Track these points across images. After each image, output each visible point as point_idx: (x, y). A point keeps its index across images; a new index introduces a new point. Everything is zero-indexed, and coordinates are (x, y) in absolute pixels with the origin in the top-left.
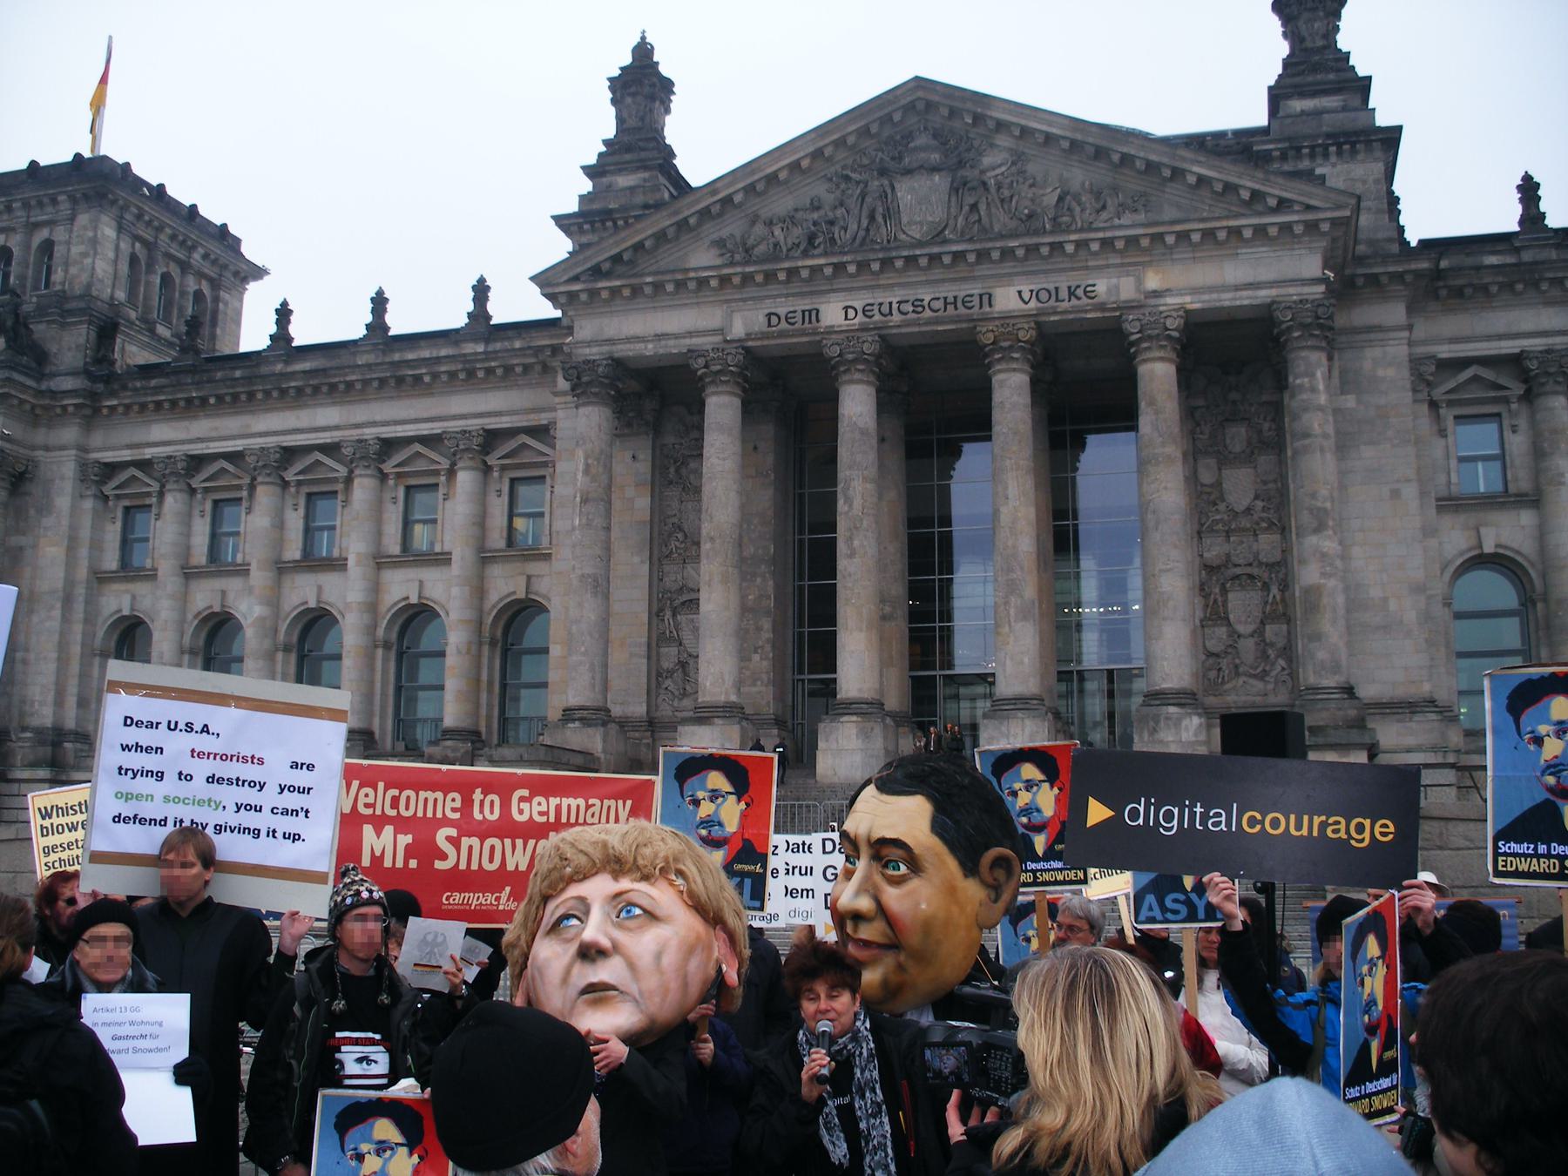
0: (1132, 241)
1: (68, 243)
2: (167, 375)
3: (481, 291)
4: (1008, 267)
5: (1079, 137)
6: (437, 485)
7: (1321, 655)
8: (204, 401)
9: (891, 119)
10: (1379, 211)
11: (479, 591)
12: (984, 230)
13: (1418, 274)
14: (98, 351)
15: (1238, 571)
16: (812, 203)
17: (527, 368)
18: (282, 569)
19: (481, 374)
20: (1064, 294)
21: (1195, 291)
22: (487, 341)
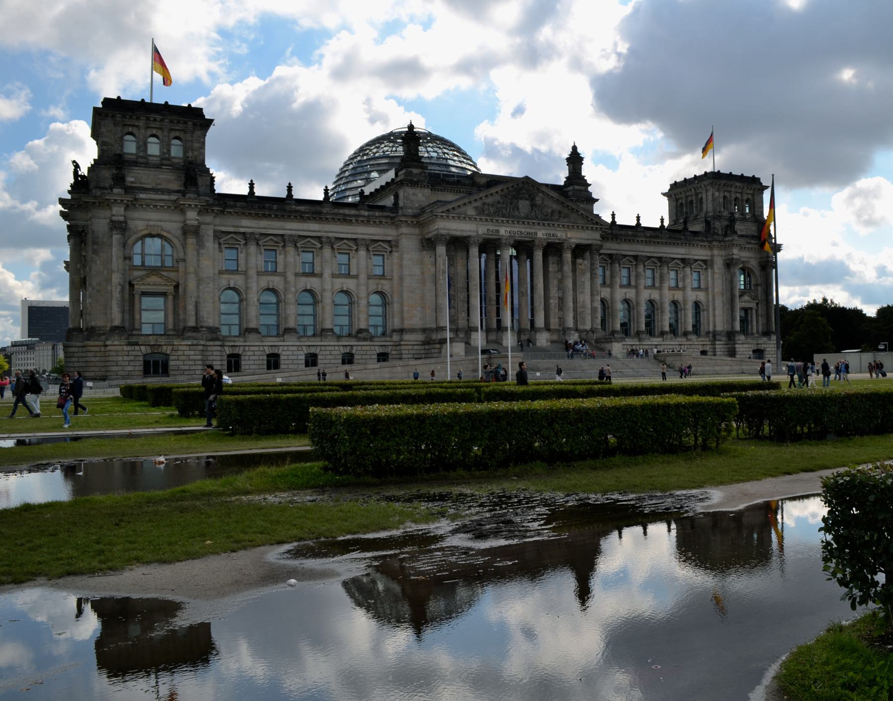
0: (568, 226)
2: (247, 202)
8: (270, 215)
9: (518, 184)
11: (368, 288)
17: (386, 222)
18: (297, 275)
21: (577, 238)
22: (368, 211)
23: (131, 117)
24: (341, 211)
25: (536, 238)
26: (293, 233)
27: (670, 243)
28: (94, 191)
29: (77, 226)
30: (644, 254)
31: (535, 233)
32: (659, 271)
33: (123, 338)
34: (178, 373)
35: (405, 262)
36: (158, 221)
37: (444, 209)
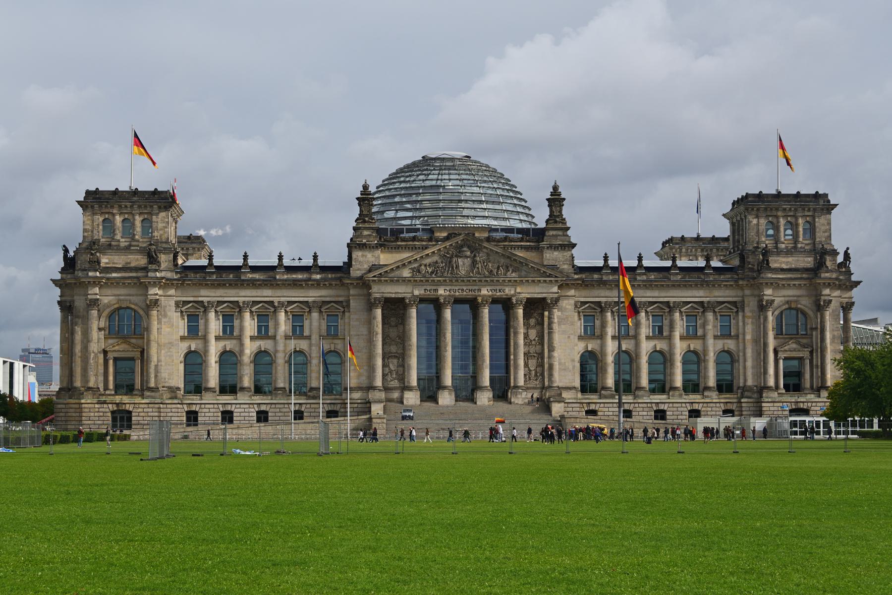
0: (516, 281)
1: (157, 222)
3: (315, 257)
4: (485, 283)
5: (504, 253)
6: (303, 315)
7: (553, 379)
10: (570, 265)
12: (479, 273)
13: (578, 284)
14: (174, 261)
15: (531, 354)
16: (437, 261)
19: (322, 285)
20: (498, 291)
22: (320, 274)
23: (106, 206)
24: (294, 276)
25: (480, 296)
26: (247, 299)
27: (679, 285)
28: (76, 272)
29: (65, 301)
30: (644, 300)
31: (480, 290)
32: (668, 318)
33: (95, 397)
34: (138, 427)
35: (351, 323)
36: (127, 296)
37: (377, 273)
